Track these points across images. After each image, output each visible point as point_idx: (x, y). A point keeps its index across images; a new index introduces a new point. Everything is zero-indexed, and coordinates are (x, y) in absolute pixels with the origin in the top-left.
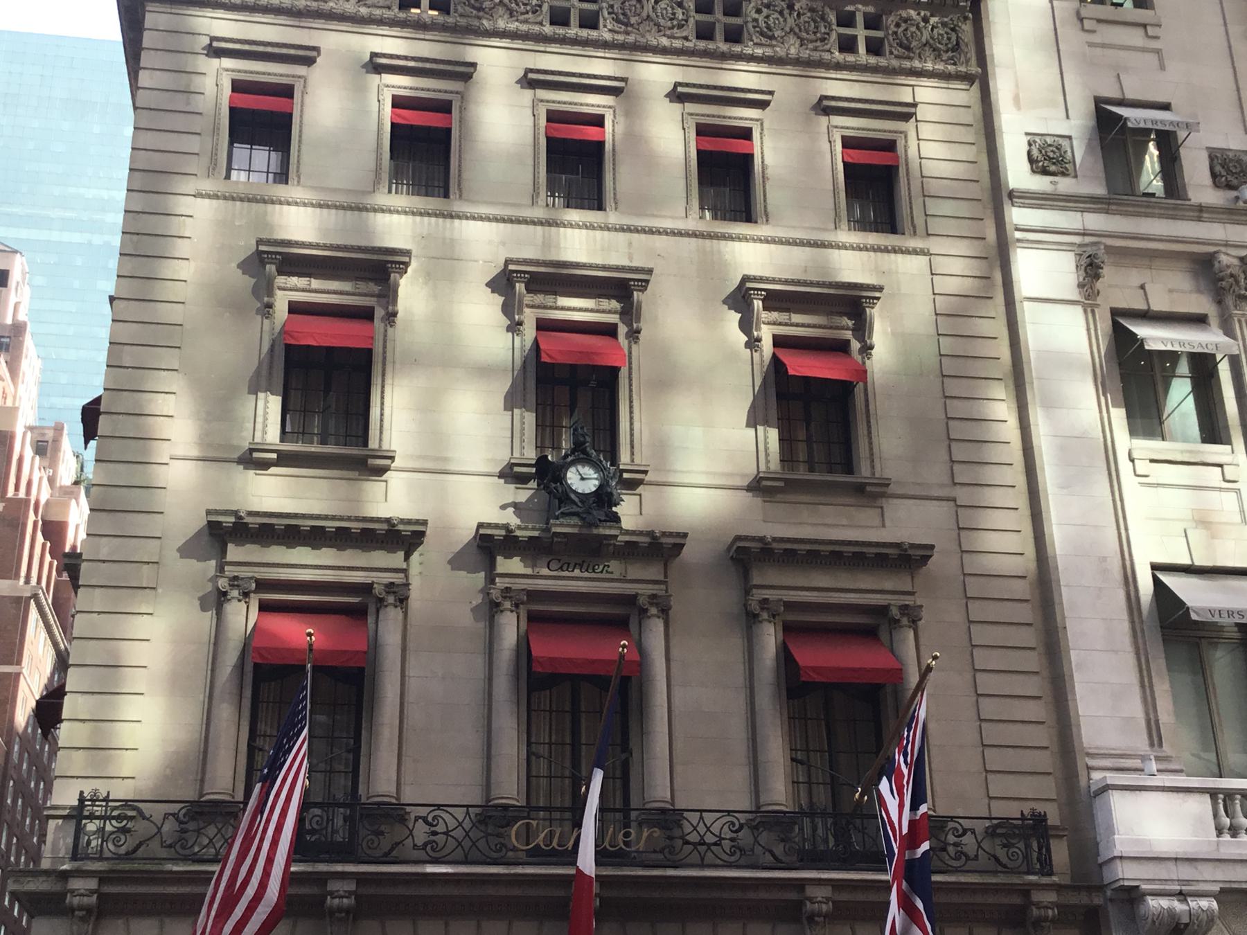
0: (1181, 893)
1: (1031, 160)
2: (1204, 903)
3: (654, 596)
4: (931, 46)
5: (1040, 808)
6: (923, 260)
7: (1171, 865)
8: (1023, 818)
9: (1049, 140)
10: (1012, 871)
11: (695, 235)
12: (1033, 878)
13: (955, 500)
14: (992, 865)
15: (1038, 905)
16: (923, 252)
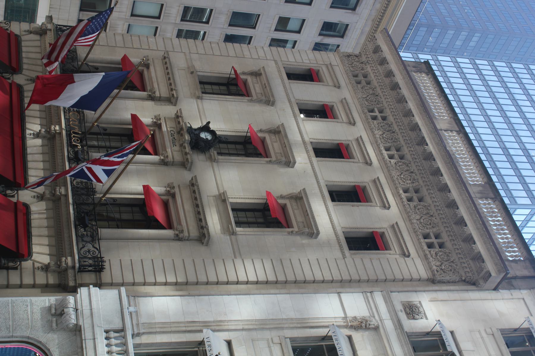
0: (77, 310)
1: (409, 302)
2: (73, 317)
3: (167, 156)
4: (442, 264)
5: (107, 265)
6: (341, 256)
7: (89, 308)
8: (101, 258)
9: (421, 309)
10: (79, 253)
11: (318, 182)
12: (77, 257)
13: (235, 257)
14: (81, 246)
15: (66, 258)
16: (344, 257)
